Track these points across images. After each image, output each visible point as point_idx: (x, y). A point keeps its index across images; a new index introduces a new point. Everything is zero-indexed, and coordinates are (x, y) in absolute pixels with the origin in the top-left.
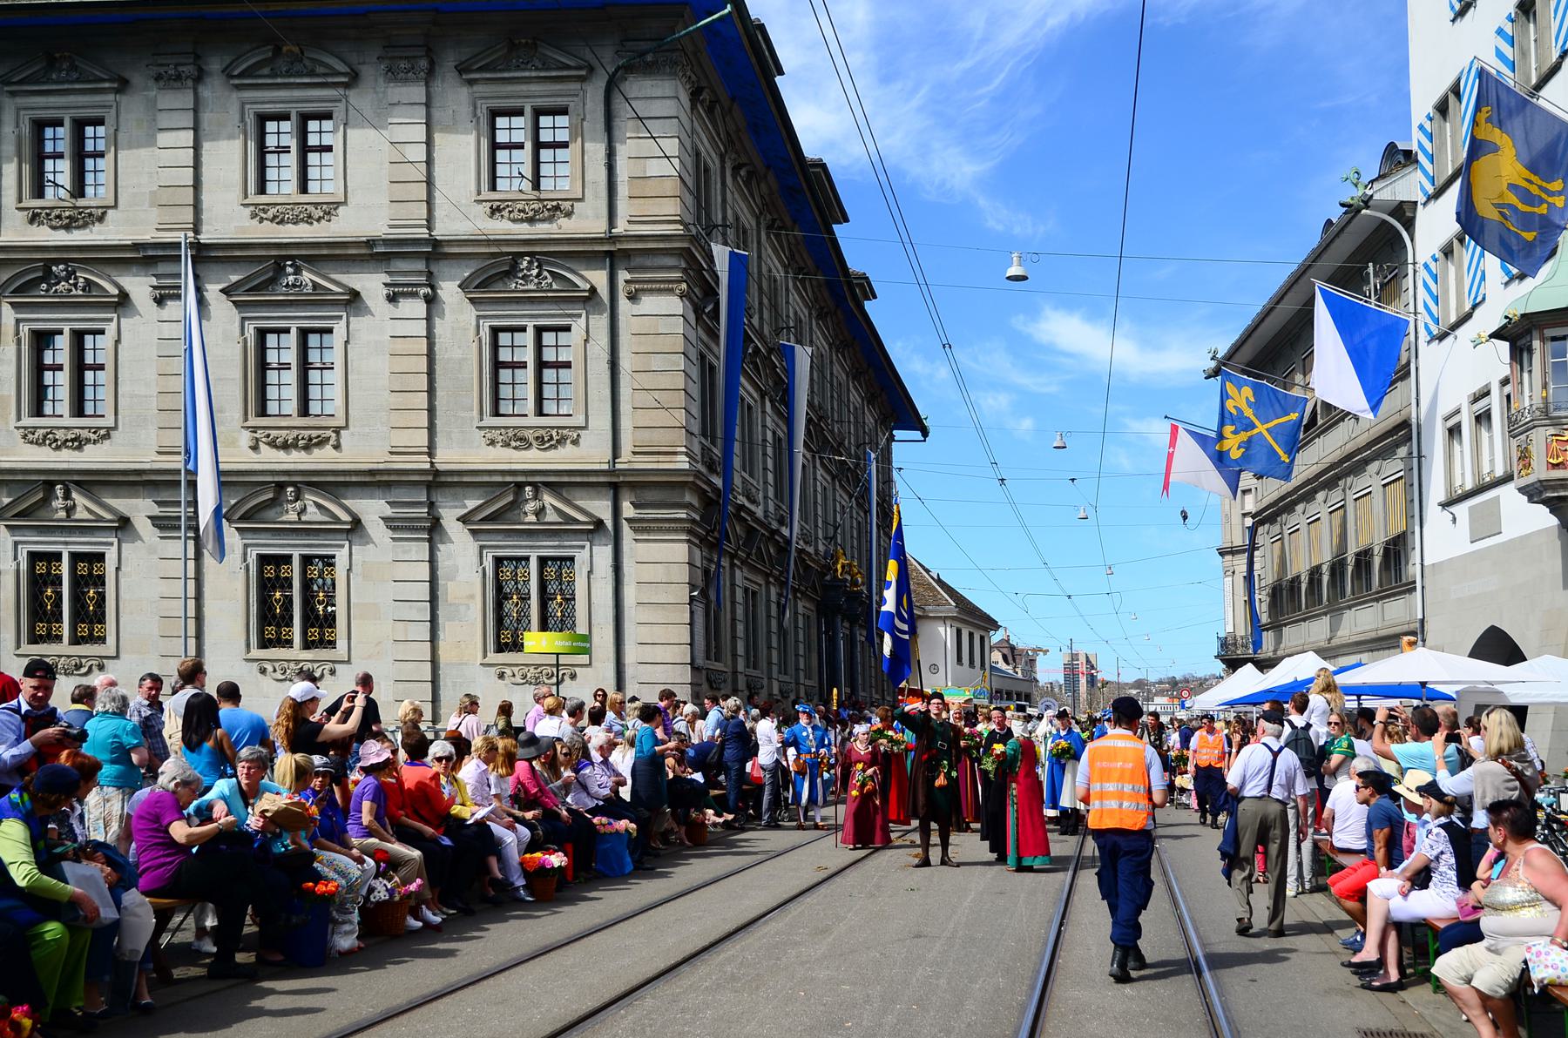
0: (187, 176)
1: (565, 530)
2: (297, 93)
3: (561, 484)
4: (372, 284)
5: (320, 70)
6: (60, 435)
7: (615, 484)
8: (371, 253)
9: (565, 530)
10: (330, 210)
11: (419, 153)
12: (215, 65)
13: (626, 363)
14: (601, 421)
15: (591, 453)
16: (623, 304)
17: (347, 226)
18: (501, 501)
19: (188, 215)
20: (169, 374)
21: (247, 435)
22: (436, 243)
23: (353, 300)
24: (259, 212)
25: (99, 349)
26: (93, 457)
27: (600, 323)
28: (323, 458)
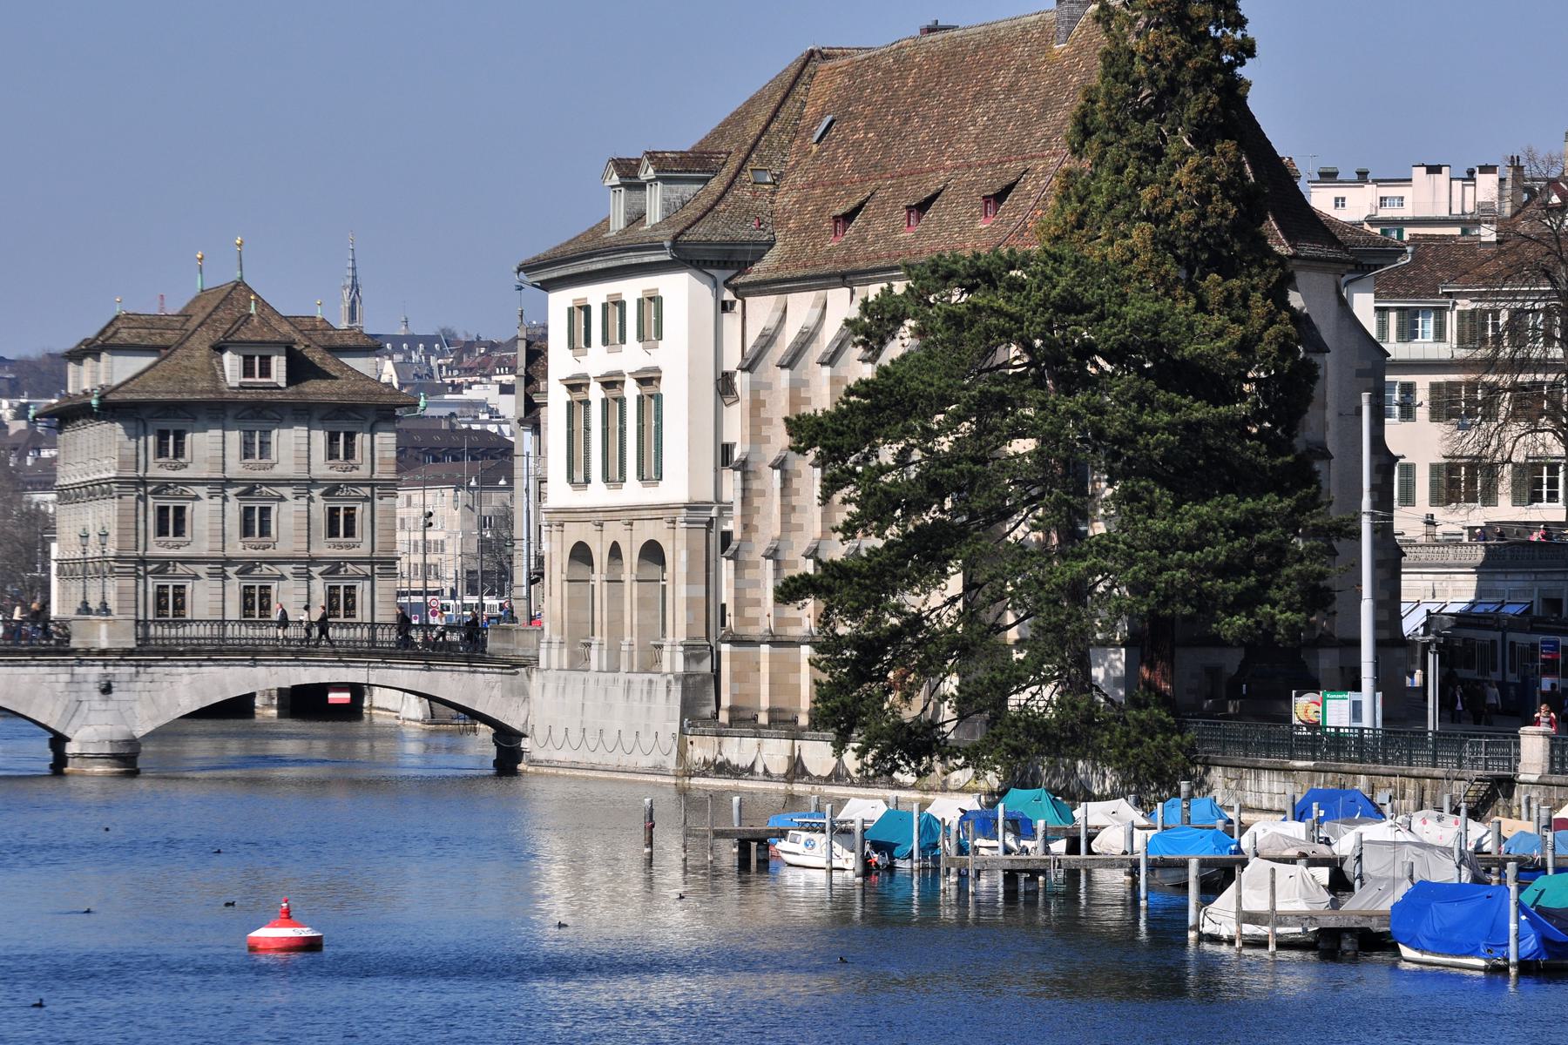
0: (220, 453)
1: (356, 577)
3: (356, 561)
4: (287, 492)
8: (287, 482)
9: (356, 577)
10: (272, 466)
11: (305, 448)
12: (230, 413)
13: (377, 521)
14: (368, 540)
15: (363, 550)
16: (377, 501)
17: (279, 471)
18: (334, 567)
20: (210, 523)
22: (313, 480)
23: (282, 499)
24: (246, 466)
25: (188, 511)
27: (368, 505)
28: (269, 552)
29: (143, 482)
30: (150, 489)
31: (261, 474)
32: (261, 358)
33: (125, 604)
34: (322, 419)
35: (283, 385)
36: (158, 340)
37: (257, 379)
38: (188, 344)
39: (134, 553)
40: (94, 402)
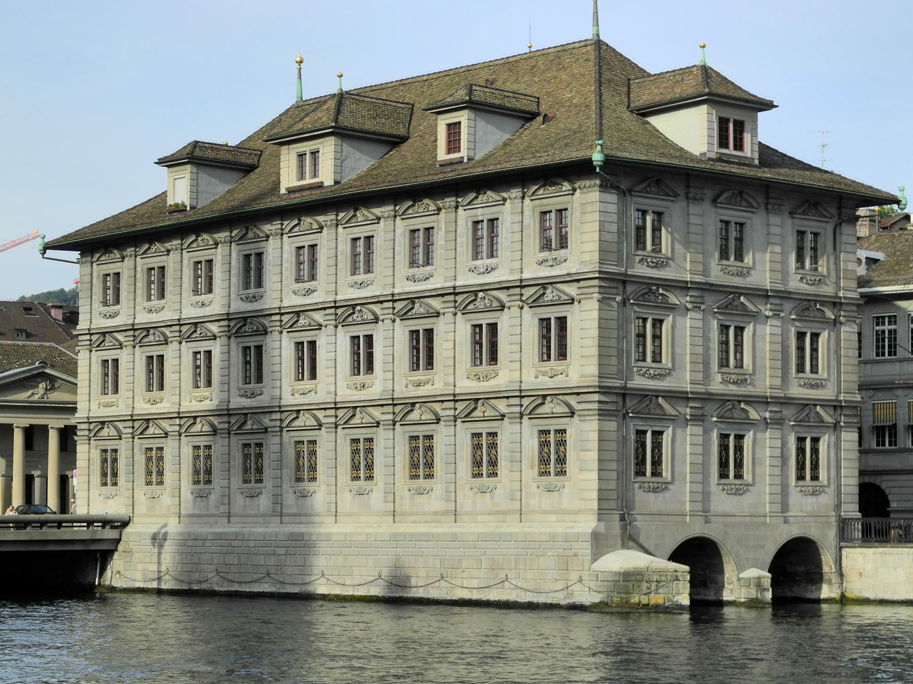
2: (736, 213)
3: (825, 404)
5: (744, 203)
6: (652, 371)
7: (836, 406)
8: (763, 295)
14: (834, 378)
15: (828, 393)
19: (700, 268)
21: (719, 375)
26: (666, 384)
29: (623, 281)
30: (630, 289)
31: (737, 281)
32: (735, 122)
33: (607, 456)
34: (792, 214)
35: (757, 162)
36: (518, 106)
37: (731, 151)
38: (605, 104)
39: (617, 383)
40: (597, 157)
